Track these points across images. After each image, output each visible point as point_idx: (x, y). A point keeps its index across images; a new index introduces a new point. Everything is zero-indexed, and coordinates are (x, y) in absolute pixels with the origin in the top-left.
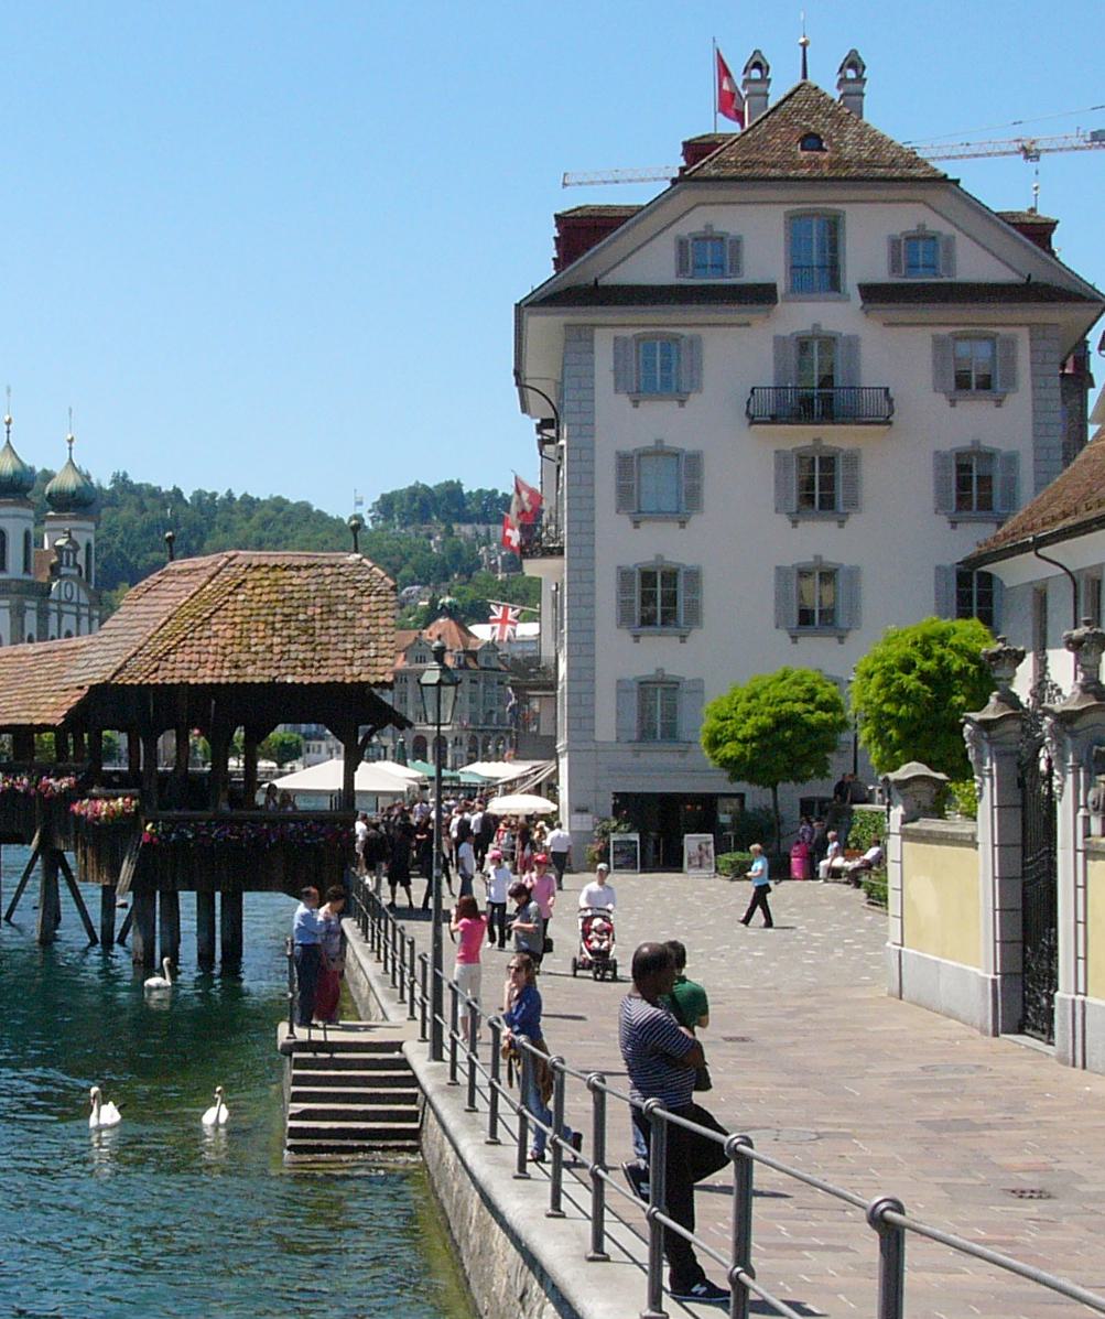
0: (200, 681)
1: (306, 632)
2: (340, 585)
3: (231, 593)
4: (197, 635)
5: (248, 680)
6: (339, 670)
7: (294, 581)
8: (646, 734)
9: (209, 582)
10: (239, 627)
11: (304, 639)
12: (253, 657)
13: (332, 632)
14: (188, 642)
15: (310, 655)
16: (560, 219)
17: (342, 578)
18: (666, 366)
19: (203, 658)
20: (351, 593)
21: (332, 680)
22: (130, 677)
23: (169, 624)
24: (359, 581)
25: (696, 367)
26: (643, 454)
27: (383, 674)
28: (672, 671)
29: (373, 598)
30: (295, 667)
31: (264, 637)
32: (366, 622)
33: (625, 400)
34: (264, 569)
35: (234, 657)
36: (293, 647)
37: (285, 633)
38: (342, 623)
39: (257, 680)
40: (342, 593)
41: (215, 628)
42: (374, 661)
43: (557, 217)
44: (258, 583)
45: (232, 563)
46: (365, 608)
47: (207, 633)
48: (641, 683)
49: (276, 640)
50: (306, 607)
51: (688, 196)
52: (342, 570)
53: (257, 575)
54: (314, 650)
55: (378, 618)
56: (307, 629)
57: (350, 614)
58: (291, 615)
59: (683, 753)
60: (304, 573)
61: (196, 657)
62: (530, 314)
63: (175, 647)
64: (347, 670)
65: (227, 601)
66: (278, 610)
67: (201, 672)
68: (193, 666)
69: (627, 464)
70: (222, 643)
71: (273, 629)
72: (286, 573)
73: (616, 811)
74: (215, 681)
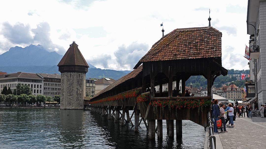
0: (164, 60)
2: (206, 34)
4: (165, 49)
5: (178, 59)
12: (179, 53)
15: (196, 52)
17: (206, 32)
24: (211, 33)
35: (174, 53)
42: (215, 52)
52: (206, 30)
53: (183, 33)
58: (191, 42)
60: (195, 32)
63: (158, 52)
64: (207, 55)
66: (188, 41)
67: (165, 58)
74: (169, 59)
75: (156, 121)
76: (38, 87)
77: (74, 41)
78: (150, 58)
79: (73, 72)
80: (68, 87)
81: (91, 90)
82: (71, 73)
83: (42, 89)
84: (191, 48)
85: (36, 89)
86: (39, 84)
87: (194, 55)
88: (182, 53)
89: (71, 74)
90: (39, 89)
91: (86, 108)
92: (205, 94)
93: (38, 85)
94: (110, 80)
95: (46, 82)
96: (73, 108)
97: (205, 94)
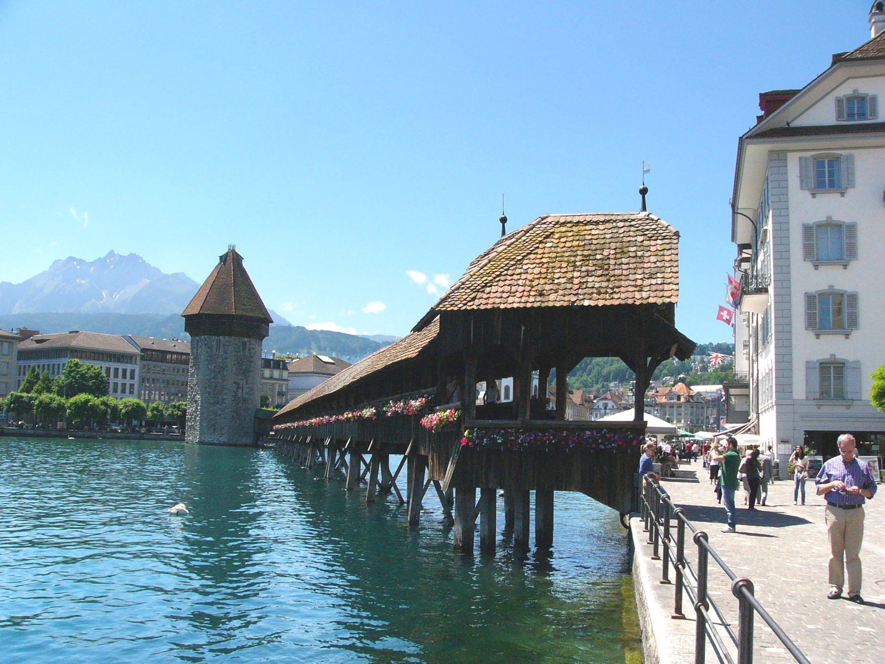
0: (509, 306)
1: (602, 268)
2: (631, 234)
3: (540, 242)
4: (510, 272)
5: (550, 304)
6: (630, 295)
7: (593, 232)
8: (824, 394)
9: (524, 235)
10: (545, 266)
11: (600, 273)
12: (555, 287)
13: (624, 267)
14: (502, 278)
15: (605, 284)
16: (762, 96)
17: (633, 229)
18: (831, 174)
19: (514, 289)
20: (640, 239)
21: (623, 302)
22: (452, 305)
23: (489, 265)
24: (647, 230)
25: (851, 173)
26: (819, 226)
27: (669, 297)
28: (841, 355)
29: (659, 242)
30: (592, 293)
31: (566, 272)
32: (653, 259)
33: (807, 194)
34: (569, 225)
35: (540, 288)
36: (590, 279)
37: (584, 269)
38: (633, 260)
39: (558, 304)
40: (633, 239)
41: (525, 267)
42: (661, 287)
43: (762, 96)
44: (563, 235)
45: (543, 222)
46: (652, 249)
47: (518, 271)
48: (821, 363)
49: (576, 274)
50: (603, 249)
51: (842, 72)
52: (633, 223)
53: (563, 229)
54: (608, 280)
55: (663, 255)
56: (603, 265)
57: (639, 254)
58: (590, 255)
59: (848, 406)
60: (601, 227)
61: (507, 288)
62: (749, 143)
64: (637, 295)
65: (538, 248)
66: (579, 253)
67: (510, 300)
68: (505, 295)
69: (808, 230)
70: (530, 277)
71: (575, 266)
72: (587, 227)
73: (807, 442)
74: (522, 305)
75: (478, 490)
76: (124, 376)
77: (232, 243)
78: (465, 300)
79: (225, 335)
80: (211, 379)
81: (277, 390)
82: (221, 338)
83: (136, 381)
84: (588, 274)
85: (120, 380)
86: (129, 367)
87: (599, 293)
88: (563, 286)
89: (219, 343)
90: (128, 381)
91: (260, 443)
92: (605, 408)
93: (124, 371)
94: (333, 362)
95: (146, 362)
96: (224, 439)
97: (605, 408)
